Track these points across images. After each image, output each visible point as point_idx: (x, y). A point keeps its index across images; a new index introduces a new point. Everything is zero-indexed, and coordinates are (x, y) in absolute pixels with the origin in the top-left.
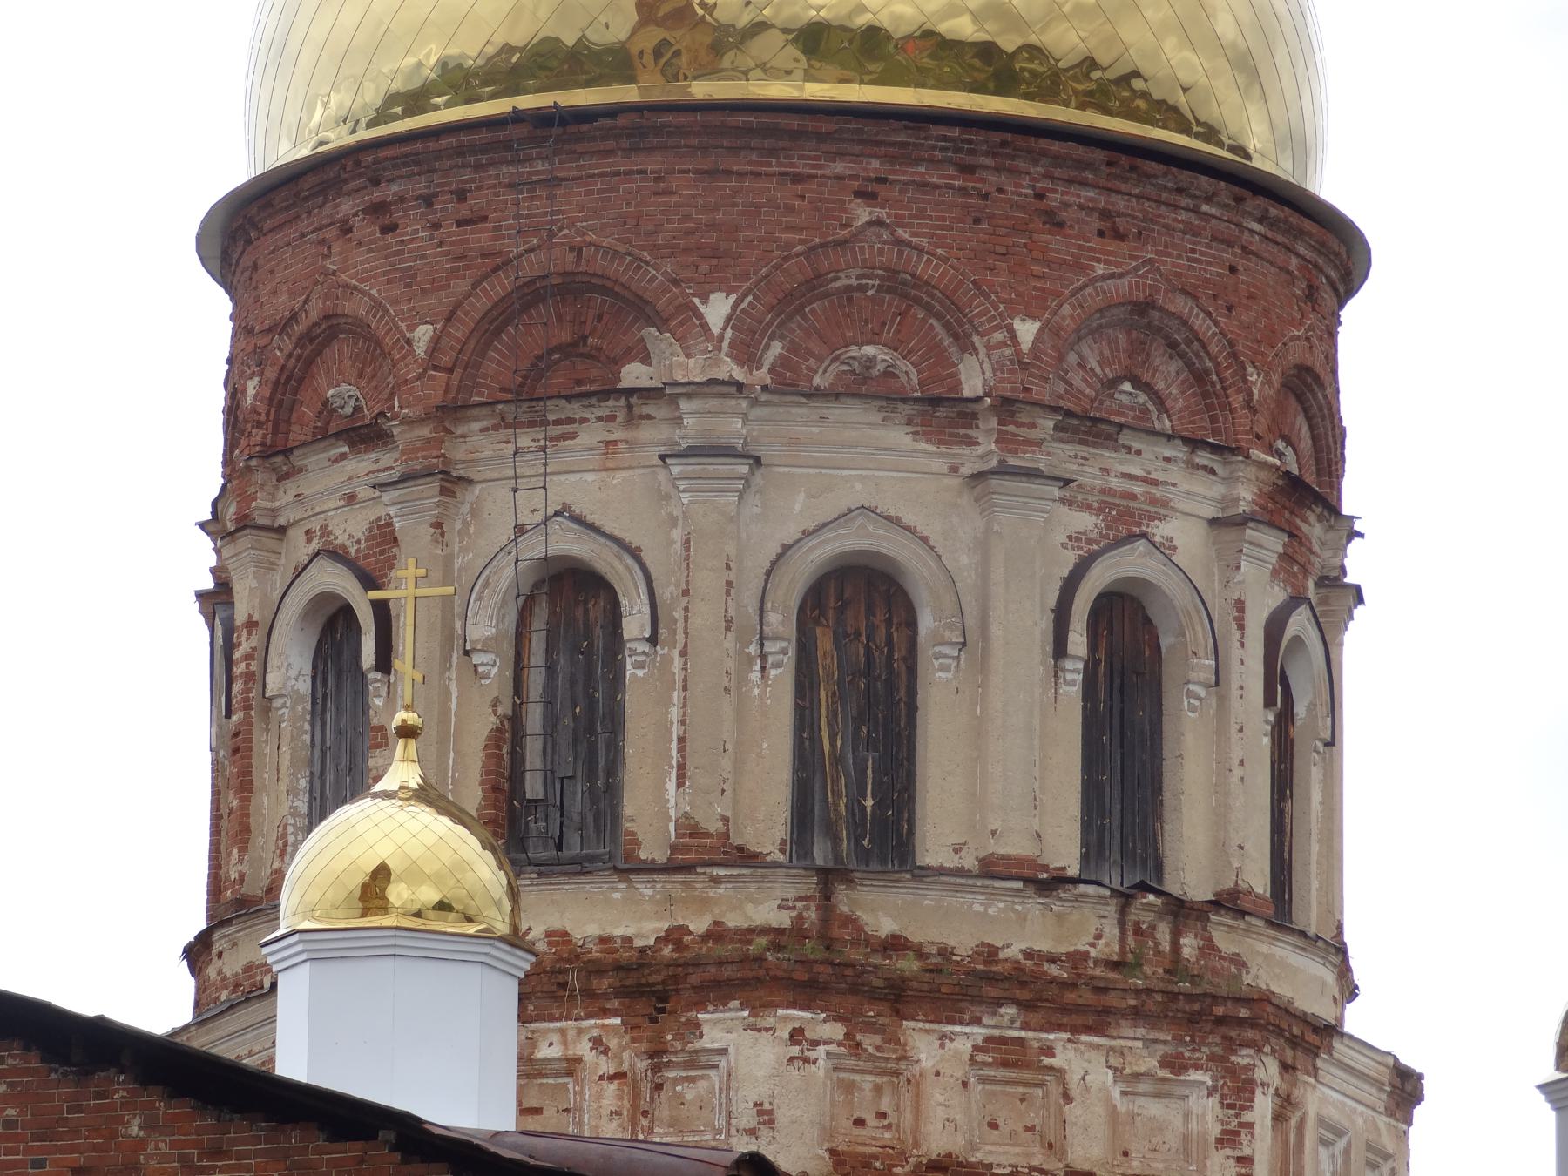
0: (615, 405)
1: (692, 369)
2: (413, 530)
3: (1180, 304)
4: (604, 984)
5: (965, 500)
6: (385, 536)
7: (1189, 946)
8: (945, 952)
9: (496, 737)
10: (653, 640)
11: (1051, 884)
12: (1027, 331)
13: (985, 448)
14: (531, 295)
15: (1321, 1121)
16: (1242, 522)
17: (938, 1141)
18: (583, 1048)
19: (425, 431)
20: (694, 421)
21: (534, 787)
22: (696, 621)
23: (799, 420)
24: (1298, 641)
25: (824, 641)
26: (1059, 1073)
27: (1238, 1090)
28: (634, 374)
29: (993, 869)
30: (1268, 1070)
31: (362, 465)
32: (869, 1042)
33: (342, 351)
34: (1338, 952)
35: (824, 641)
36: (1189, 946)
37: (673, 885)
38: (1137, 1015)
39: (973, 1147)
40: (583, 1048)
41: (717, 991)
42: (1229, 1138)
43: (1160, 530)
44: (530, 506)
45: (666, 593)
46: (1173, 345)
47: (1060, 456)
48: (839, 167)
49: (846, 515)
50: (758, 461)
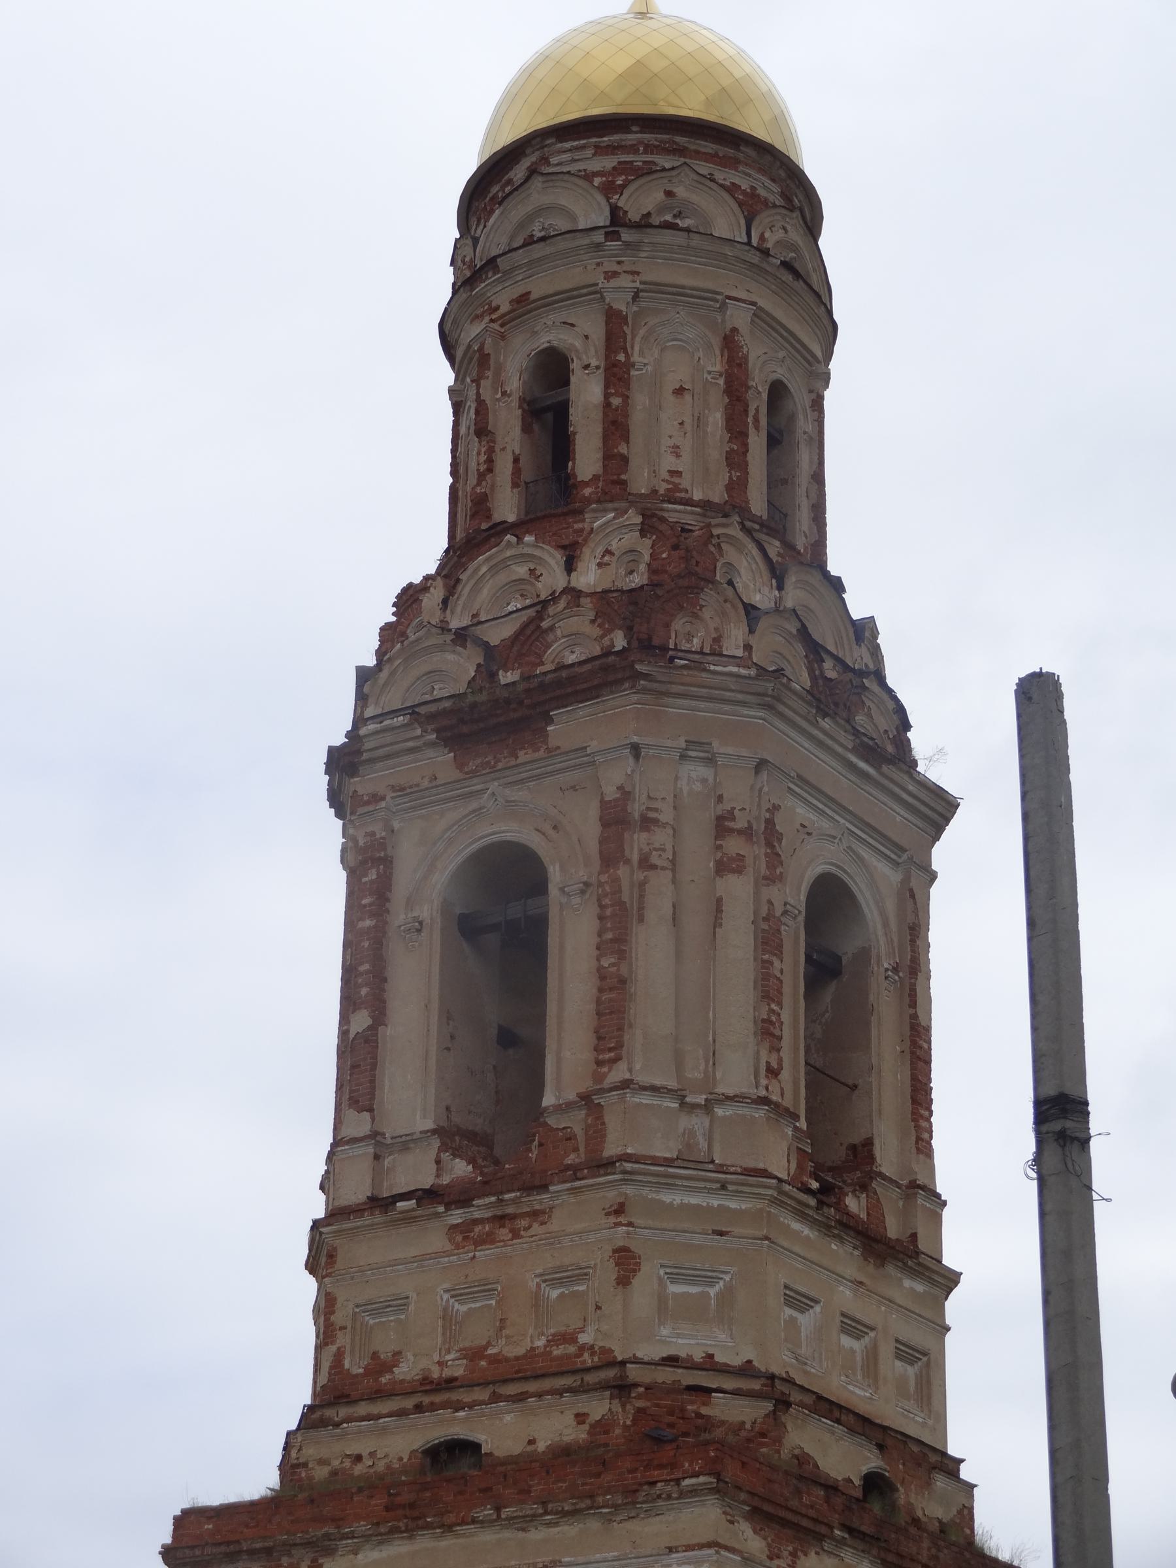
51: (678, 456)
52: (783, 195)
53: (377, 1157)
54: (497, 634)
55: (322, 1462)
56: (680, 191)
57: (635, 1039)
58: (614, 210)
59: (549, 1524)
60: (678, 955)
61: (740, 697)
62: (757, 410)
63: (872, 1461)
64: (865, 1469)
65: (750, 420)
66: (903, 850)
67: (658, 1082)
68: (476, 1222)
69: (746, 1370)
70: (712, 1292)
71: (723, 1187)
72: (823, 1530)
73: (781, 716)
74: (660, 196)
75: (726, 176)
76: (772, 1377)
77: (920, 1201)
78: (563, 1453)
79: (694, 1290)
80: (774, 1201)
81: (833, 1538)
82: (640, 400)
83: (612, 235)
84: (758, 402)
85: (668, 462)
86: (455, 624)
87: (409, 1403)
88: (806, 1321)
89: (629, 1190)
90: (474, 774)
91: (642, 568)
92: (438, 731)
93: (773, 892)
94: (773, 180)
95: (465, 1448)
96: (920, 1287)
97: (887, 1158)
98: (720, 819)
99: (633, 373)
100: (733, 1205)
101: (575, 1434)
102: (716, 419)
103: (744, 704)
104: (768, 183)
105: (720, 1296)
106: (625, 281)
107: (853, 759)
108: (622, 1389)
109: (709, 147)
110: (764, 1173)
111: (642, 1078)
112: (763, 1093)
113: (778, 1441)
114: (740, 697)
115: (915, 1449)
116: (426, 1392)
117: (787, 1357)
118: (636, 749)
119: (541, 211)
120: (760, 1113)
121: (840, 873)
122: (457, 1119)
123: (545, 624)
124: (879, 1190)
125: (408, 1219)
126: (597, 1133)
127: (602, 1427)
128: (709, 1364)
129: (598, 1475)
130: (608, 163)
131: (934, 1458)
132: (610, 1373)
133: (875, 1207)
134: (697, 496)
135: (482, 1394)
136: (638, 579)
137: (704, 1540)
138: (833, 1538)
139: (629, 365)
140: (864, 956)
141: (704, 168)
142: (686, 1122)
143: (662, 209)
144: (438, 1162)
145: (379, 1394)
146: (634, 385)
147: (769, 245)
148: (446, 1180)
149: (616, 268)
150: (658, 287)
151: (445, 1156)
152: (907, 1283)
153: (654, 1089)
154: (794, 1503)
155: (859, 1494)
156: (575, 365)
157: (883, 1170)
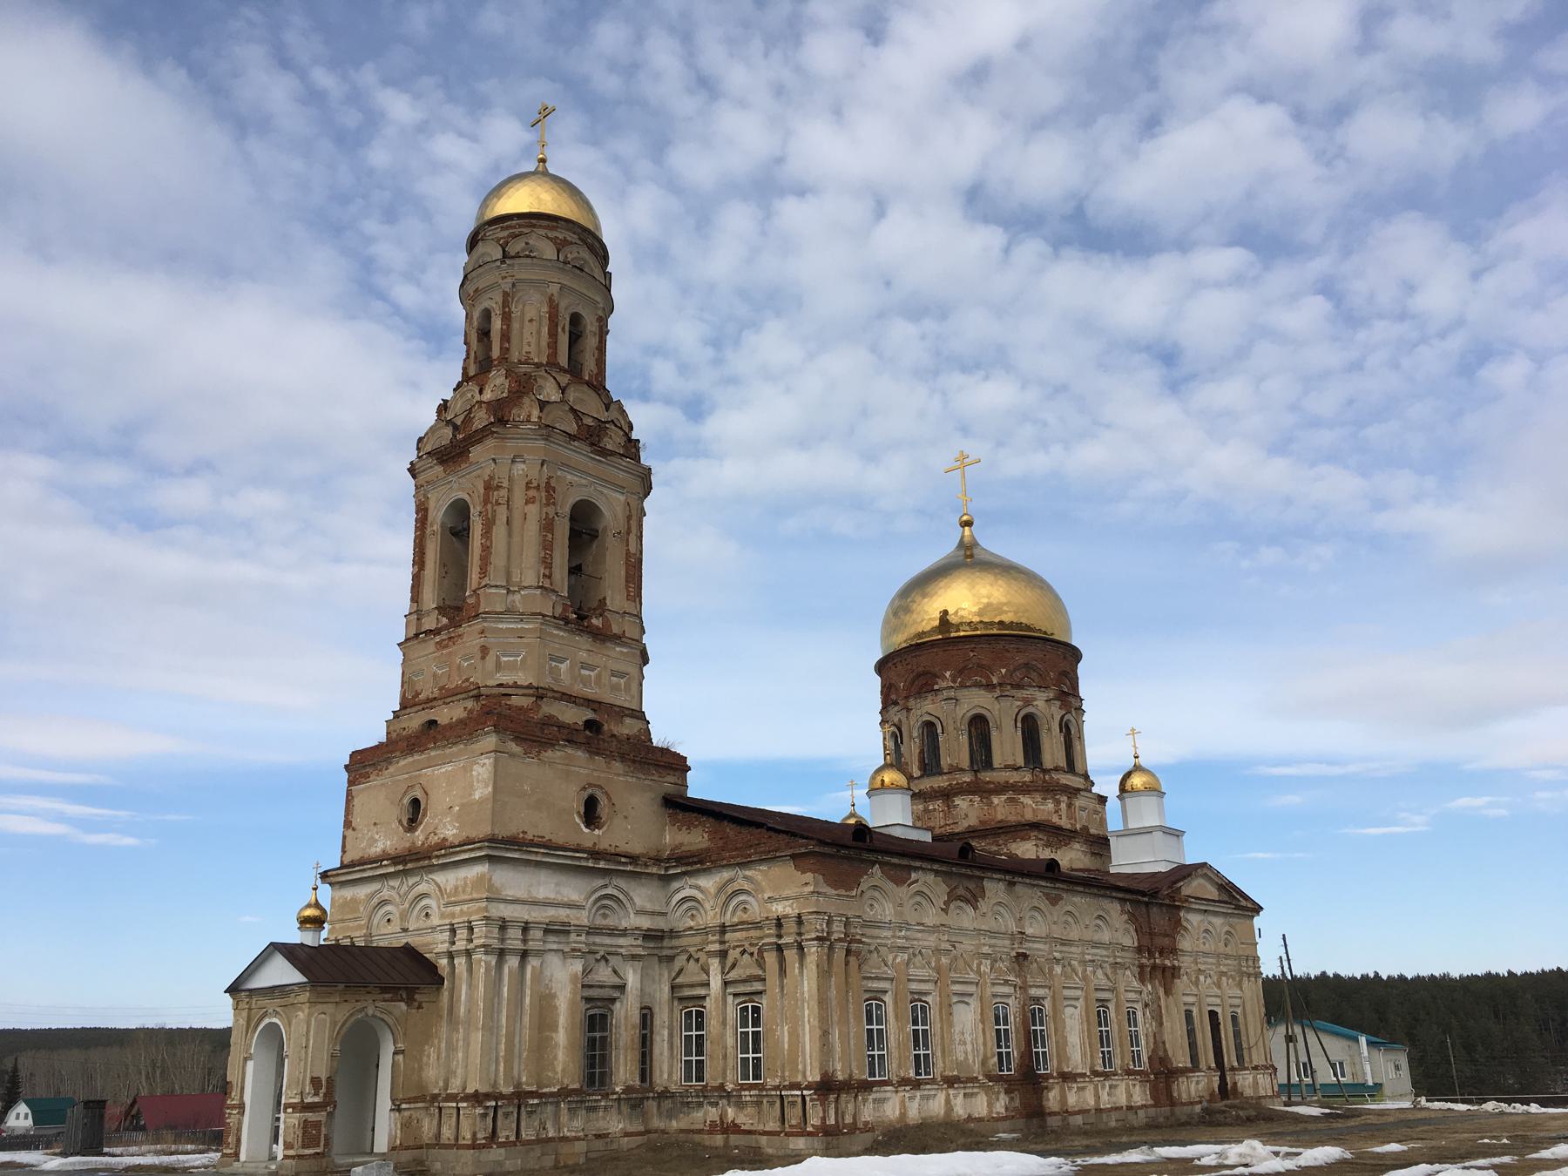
0: (933, 693)
1: (944, 685)
2: (904, 720)
3: (1034, 663)
4: (938, 795)
5: (996, 702)
6: (900, 720)
7: (1047, 777)
8: (999, 783)
9: (920, 753)
10: (943, 733)
11: (1017, 769)
12: (1003, 671)
13: (998, 693)
14: (919, 675)
15: (1080, 807)
16: (1050, 700)
17: (999, 817)
18: (937, 807)
19: (903, 701)
20: (945, 694)
21: (927, 762)
22: (949, 728)
23: (965, 692)
24: (1068, 720)
25: (973, 730)
26: (1022, 803)
27: (1058, 803)
28: (936, 687)
29: (1007, 767)
30: (1065, 798)
31: (896, 708)
32: (984, 801)
33: (893, 689)
34: (1086, 776)
35: (973, 730)
36: (1047, 777)
37: (949, 776)
38: (1036, 791)
39: (1006, 817)
40: (937, 807)
41: (956, 794)
42: (1056, 812)
43: (1035, 703)
44: (919, 712)
45: (944, 724)
46: (1034, 670)
47: (1014, 692)
48: (968, 646)
49: (974, 708)
50: (957, 700)
51: (530, 346)
52: (580, 239)
53: (418, 619)
54: (458, 421)
55: (395, 731)
56: (531, 242)
57: (491, 569)
58: (504, 251)
59: (450, 748)
60: (510, 535)
61: (533, 437)
62: (564, 325)
63: (590, 715)
64: (585, 719)
65: (560, 330)
66: (624, 488)
67: (498, 584)
68: (444, 640)
69: (530, 686)
70: (519, 659)
71: (522, 621)
72: (554, 742)
73: (554, 443)
74: (524, 244)
75: (552, 234)
76: (537, 688)
77: (627, 618)
78: (461, 722)
79: (512, 659)
80: (542, 624)
81: (560, 745)
82: (516, 326)
83: (503, 262)
84: (565, 321)
85: (526, 348)
86: (449, 418)
87: (421, 707)
88: (563, 667)
89: (485, 624)
90: (449, 474)
91: (506, 391)
92: (437, 459)
93: (551, 510)
94: (574, 233)
95: (433, 723)
96: (625, 650)
97: (616, 600)
98: (527, 483)
99: (513, 315)
100: (526, 627)
101: (464, 715)
102: (545, 330)
103: (536, 439)
104: (571, 234)
105: (521, 660)
106: (509, 280)
107: (593, 456)
108: (477, 697)
109: (545, 223)
110: (540, 614)
111: (493, 583)
112: (541, 584)
113: (538, 711)
114: (533, 437)
115: (618, 709)
116: (425, 703)
117: (549, 680)
118: (494, 460)
119: (483, 255)
120: (538, 592)
121: (590, 499)
122: (447, 603)
123: (472, 416)
124: (609, 616)
125: (424, 641)
126: (478, 603)
127: (471, 712)
128: (515, 686)
129: (464, 729)
130: (505, 233)
131: (627, 712)
132: (475, 692)
133: (607, 624)
134: (536, 360)
135: (440, 702)
136: (505, 395)
137: (491, 750)
138: (560, 745)
139: (510, 312)
140: (605, 529)
141: (542, 232)
142: (511, 597)
143: (523, 250)
144: (437, 619)
145: (415, 705)
146: (513, 321)
147: (569, 260)
148: (440, 625)
149: (505, 275)
150: (521, 281)
151: (440, 617)
152: (618, 649)
153: (496, 586)
154: (539, 734)
155: (582, 728)
156: (493, 314)
157: (610, 608)
